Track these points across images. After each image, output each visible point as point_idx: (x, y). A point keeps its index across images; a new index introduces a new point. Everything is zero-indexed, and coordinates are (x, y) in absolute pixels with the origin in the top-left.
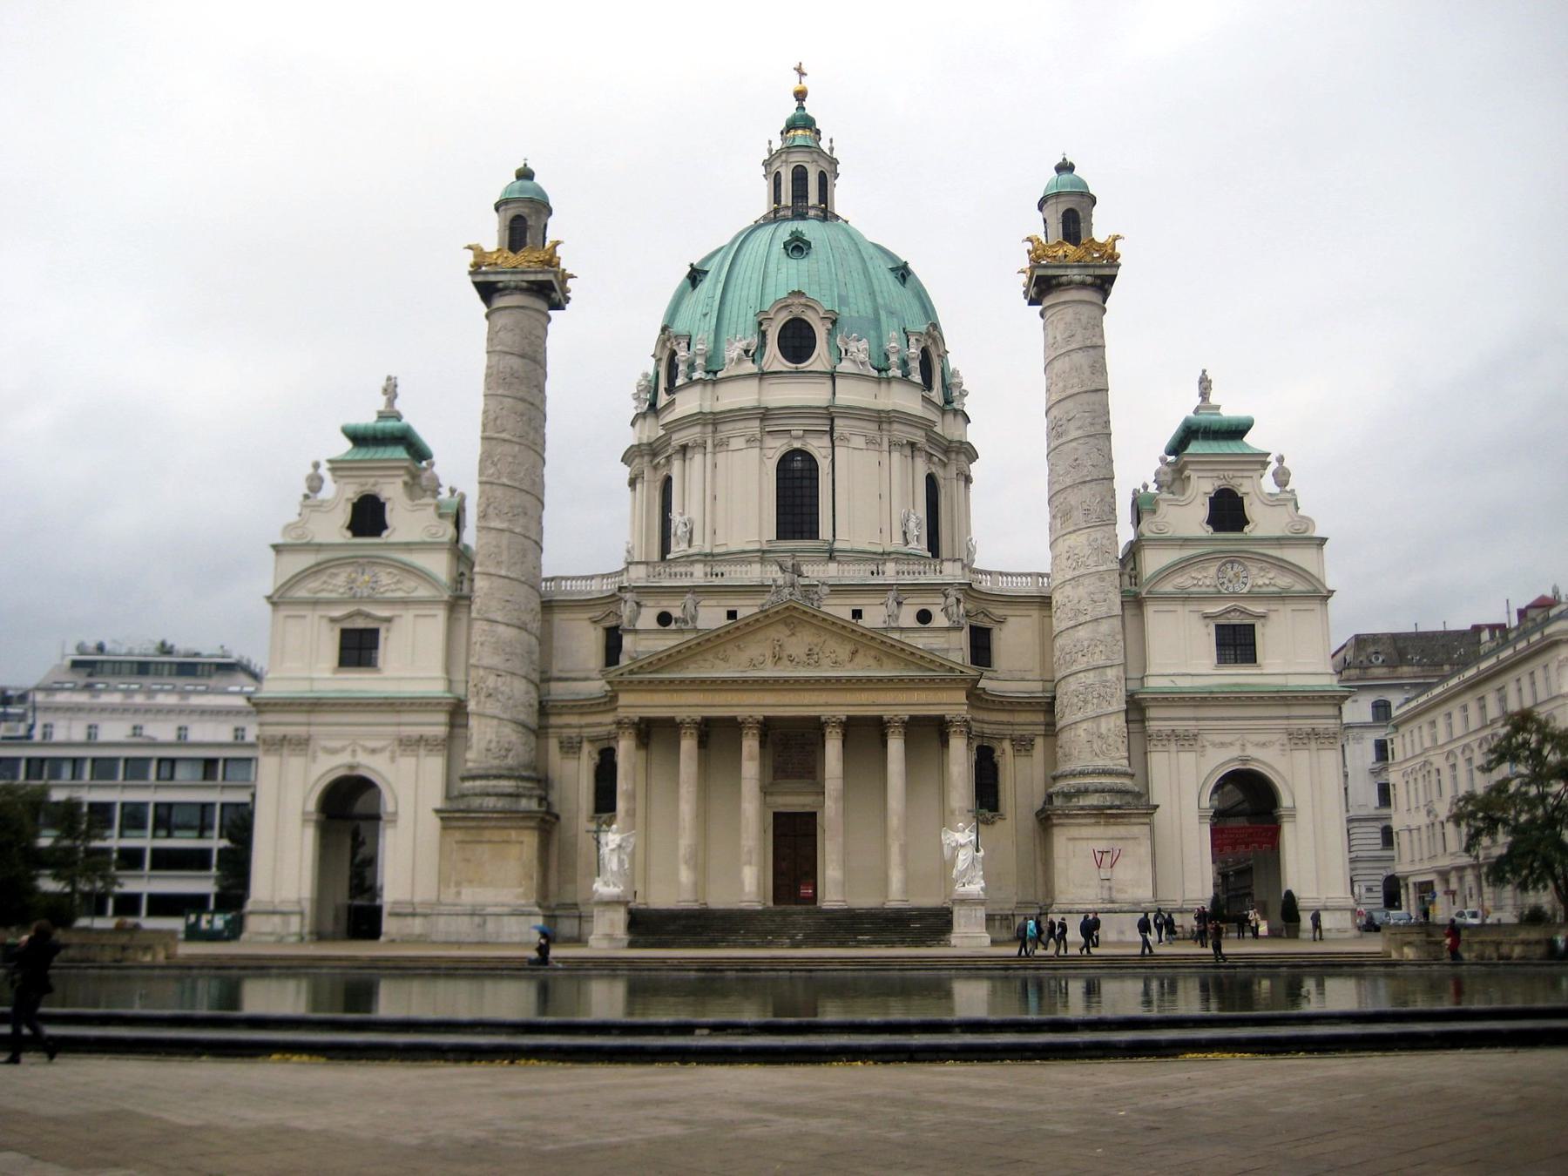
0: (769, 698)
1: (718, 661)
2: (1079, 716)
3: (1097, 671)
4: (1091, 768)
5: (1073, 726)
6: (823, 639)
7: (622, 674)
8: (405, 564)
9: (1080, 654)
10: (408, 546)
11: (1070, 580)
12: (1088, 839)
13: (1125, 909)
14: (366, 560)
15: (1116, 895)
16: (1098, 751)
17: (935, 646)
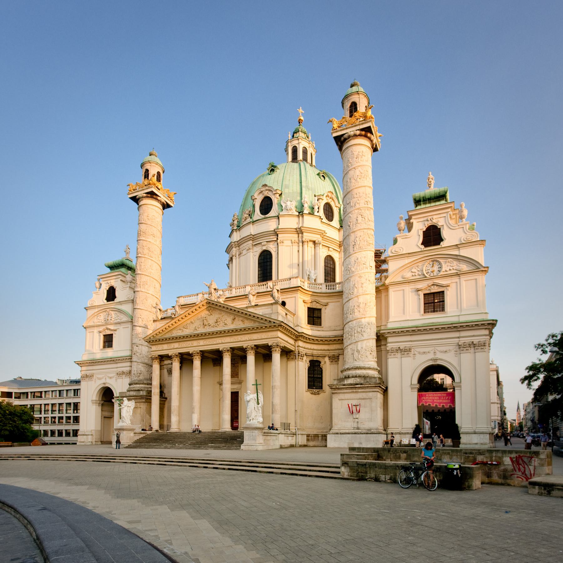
0: (202, 342)
1: (185, 329)
2: (349, 342)
3: (357, 320)
4: (352, 366)
5: (347, 348)
6: (222, 315)
7: (150, 338)
8: (119, 310)
9: (349, 313)
10: (120, 303)
11: (347, 279)
12: (348, 399)
13: (363, 432)
14: (109, 309)
15: (360, 426)
16: (355, 358)
17: (267, 313)
